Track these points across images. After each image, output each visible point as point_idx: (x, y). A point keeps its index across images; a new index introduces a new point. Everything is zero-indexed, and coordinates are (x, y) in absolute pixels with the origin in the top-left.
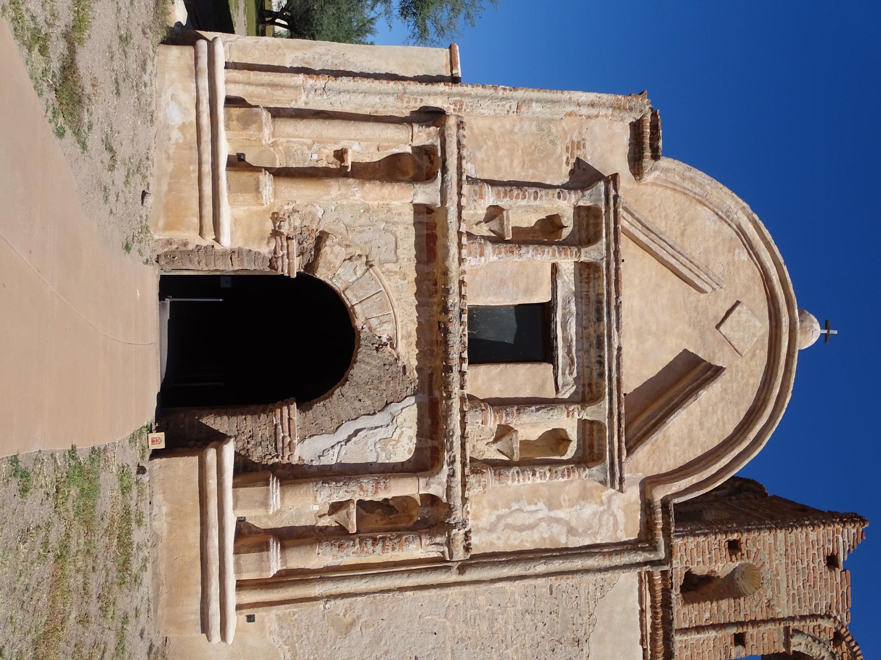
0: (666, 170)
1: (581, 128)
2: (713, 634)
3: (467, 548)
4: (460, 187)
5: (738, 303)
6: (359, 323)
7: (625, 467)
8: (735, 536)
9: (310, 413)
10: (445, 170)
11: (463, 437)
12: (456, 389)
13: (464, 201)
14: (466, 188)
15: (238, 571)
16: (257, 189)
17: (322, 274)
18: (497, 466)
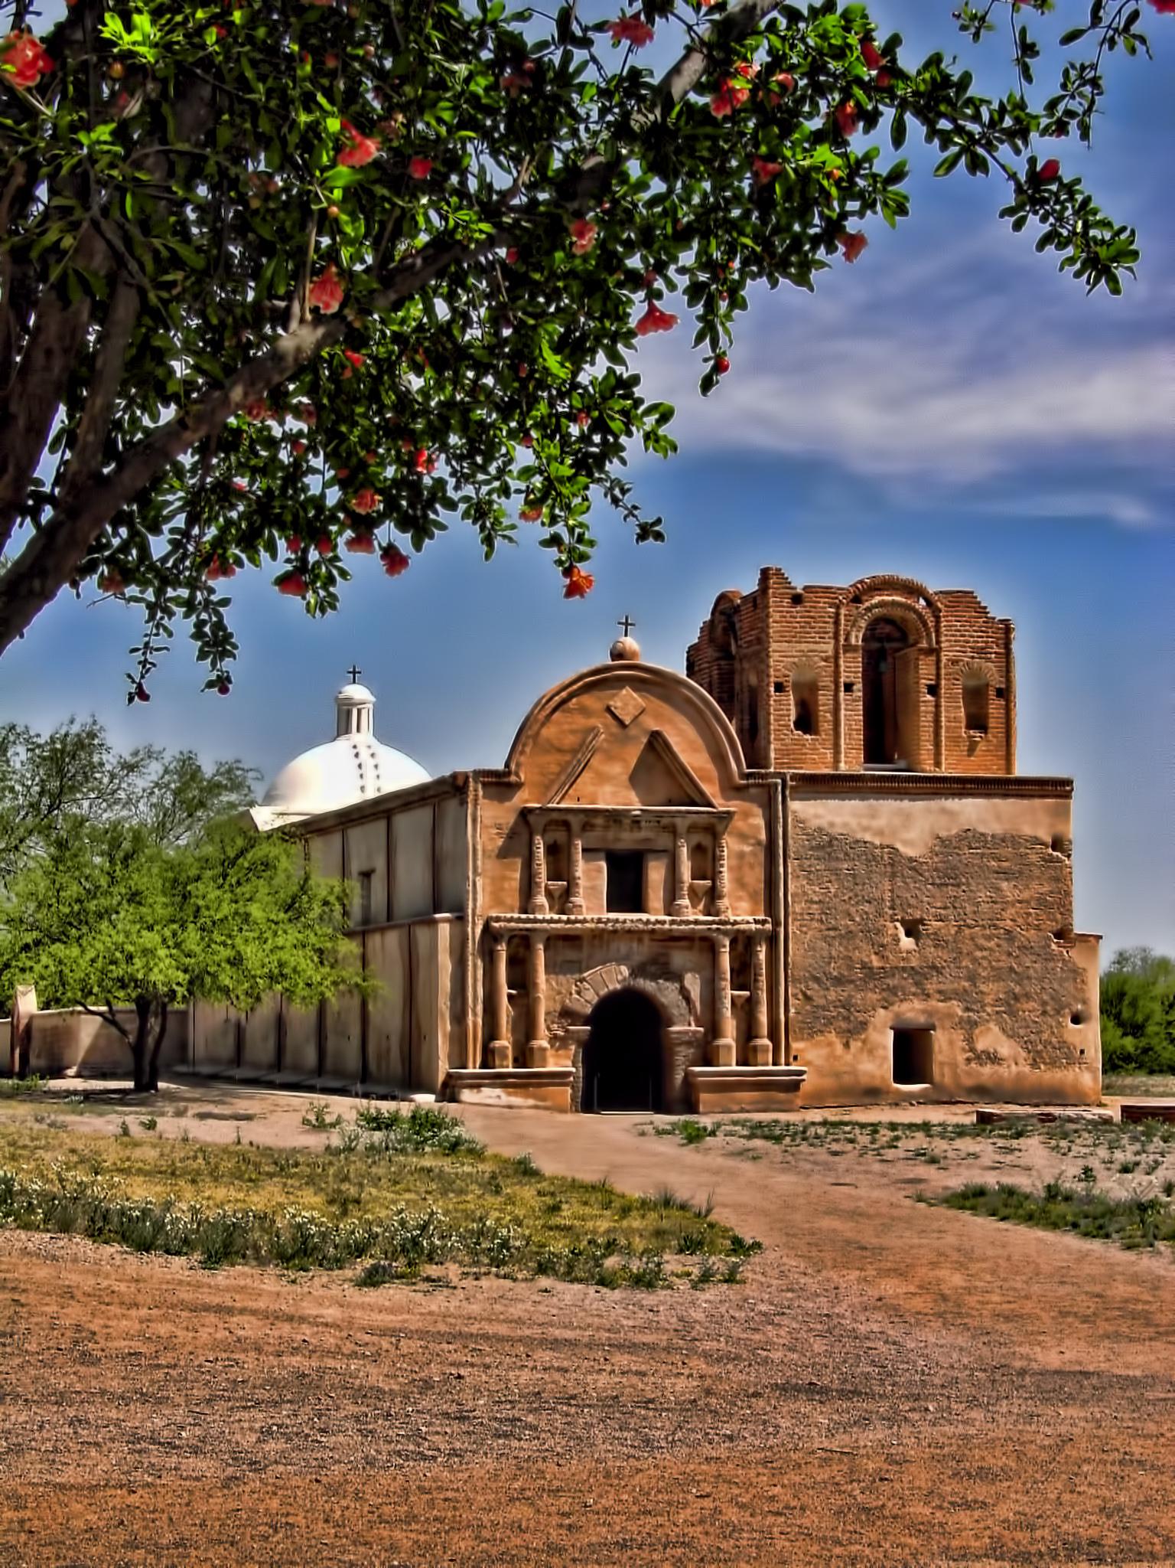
0: (518, 765)
1: (487, 827)
2: (843, 712)
3: (764, 922)
4: (536, 921)
5: (608, 710)
6: (618, 986)
7: (721, 809)
8: (772, 689)
9: (675, 1020)
10: (527, 930)
11: (696, 922)
12: (667, 926)
13: (548, 917)
14: (540, 917)
15: (767, 1064)
16: (544, 1050)
17: (589, 1010)
18: (713, 895)
